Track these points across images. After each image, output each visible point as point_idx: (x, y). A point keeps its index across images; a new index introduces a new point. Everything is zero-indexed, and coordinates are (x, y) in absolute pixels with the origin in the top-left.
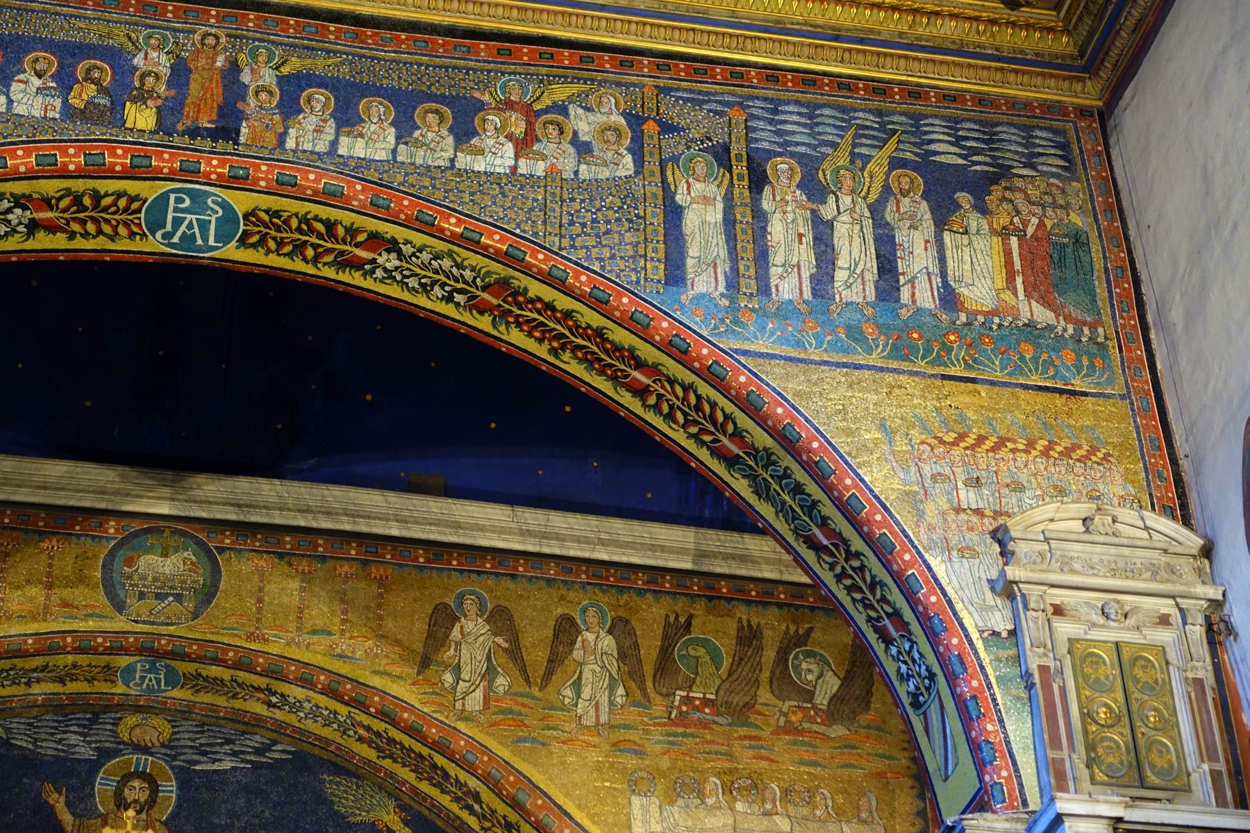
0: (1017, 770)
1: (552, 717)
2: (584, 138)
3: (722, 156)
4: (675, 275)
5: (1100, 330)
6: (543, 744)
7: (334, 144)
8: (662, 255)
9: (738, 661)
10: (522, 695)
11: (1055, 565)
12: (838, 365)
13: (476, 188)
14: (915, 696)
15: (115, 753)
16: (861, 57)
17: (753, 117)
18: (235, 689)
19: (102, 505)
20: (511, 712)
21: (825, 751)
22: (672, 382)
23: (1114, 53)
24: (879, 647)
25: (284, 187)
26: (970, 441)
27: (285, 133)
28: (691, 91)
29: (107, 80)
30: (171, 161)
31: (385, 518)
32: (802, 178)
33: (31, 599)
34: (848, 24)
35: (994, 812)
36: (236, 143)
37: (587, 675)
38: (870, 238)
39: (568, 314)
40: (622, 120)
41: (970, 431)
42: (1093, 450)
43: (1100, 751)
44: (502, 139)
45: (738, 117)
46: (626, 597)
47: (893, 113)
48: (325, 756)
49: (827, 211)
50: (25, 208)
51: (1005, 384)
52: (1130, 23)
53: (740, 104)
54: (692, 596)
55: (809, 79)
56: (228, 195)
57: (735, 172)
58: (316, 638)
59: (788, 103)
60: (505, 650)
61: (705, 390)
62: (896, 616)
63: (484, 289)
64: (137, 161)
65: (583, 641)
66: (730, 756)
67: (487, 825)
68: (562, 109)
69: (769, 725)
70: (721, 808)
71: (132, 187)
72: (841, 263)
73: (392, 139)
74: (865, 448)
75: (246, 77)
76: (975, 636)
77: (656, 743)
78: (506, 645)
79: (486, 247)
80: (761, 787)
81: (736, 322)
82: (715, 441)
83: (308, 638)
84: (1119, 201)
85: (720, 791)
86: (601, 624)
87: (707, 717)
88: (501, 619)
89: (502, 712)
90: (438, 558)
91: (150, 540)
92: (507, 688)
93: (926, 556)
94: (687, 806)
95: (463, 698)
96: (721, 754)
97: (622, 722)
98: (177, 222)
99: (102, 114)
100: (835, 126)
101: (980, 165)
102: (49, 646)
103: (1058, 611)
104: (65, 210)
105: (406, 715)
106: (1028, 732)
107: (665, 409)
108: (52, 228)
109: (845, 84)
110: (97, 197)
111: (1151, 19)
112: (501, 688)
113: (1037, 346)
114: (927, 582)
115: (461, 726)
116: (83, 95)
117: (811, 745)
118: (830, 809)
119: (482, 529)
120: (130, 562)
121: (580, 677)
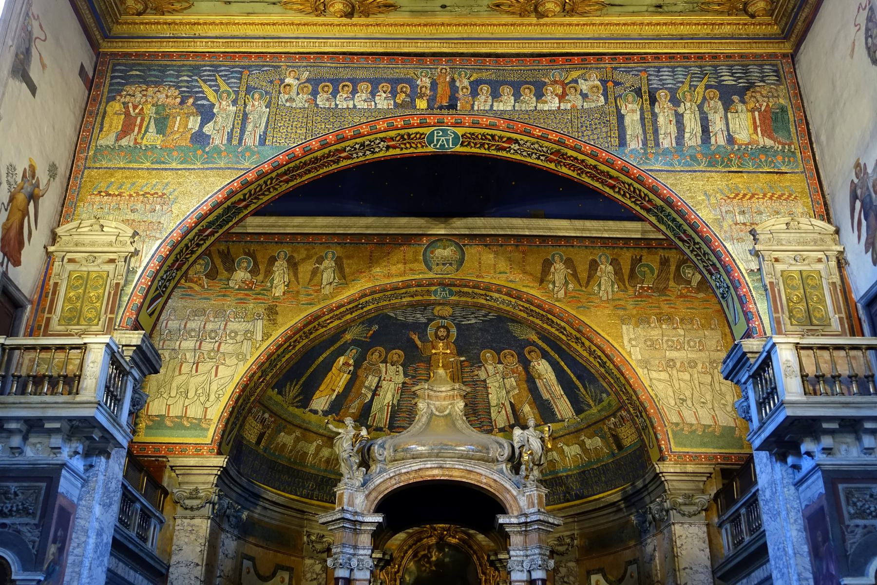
0: (762, 322)
2: (586, 92)
3: (638, 92)
4: (623, 143)
5: (793, 146)
7: (492, 106)
8: (617, 135)
9: (661, 271)
10: (579, 291)
11: (775, 243)
12: (687, 171)
13: (545, 117)
14: (723, 294)
15: (433, 320)
16: (692, 45)
17: (650, 75)
18: (473, 295)
19: (421, 232)
20: (575, 297)
21: (696, 303)
22: (624, 183)
23: (796, 31)
24: (708, 276)
25: (475, 125)
26: (740, 196)
27: (473, 104)
28: (625, 67)
29: (408, 92)
30: (434, 119)
31: (523, 228)
32: (671, 97)
33: (399, 269)
34: (686, 33)
35: (753, 338)
36: (456, 110)
37: (603, 281)
38: (698, 119)
39: (583, 161)
40: (599, 83)
41: (740, 192)
42: (790, 195)
43: (794, 312)
44: (554, 96)
45: (644, 76)
46: (616, 250)
47: (706, 66)
48: (508, 316)
49: (681, 110)
50: (384, 142)
51: (754, 172)
52: (802, 19)
53: (645, 70)
54: (641, 248)
55: (671, 56)
56: (456, 130)
57: (644, 98)
58: (501, 275)
59: (663, 67)
60: (571, 274)
61: (636, 185)
62: (714, 265)
63: (551, 154)
64: (422, 121)
66: (659, 308)
68: (576, 81)
69: (674, 295)
71: (421, 130)
72: (687, 130)
73: (513, 101)
74: (699, 203)
75: (458, 84)
76: (744, 272)
79: (551, 139)
81: (647, 159)
82: (642, 203)
83: (498, 275)
84: (800, 91)
86: (607, 262)
88: (569, 263)
89: (572, 297)
90: (544, 241)
91: (439, 244)
93: (724, 243)
98: (438, 141)
99: (408, 104)
100: (683, 75)
101: (742, 83)
102: (407, 285)
103: (777, 260)
104: (399, 141)
106: (766, 307)
107: (622, 192)
108: (394, 147)
109: (686, 57)
110: (409, 135)
111: (810, 17)
113: (767, 155)
114: (725, 253)
115: (557, 303)
119: (559, 229)
120: (432, 252)
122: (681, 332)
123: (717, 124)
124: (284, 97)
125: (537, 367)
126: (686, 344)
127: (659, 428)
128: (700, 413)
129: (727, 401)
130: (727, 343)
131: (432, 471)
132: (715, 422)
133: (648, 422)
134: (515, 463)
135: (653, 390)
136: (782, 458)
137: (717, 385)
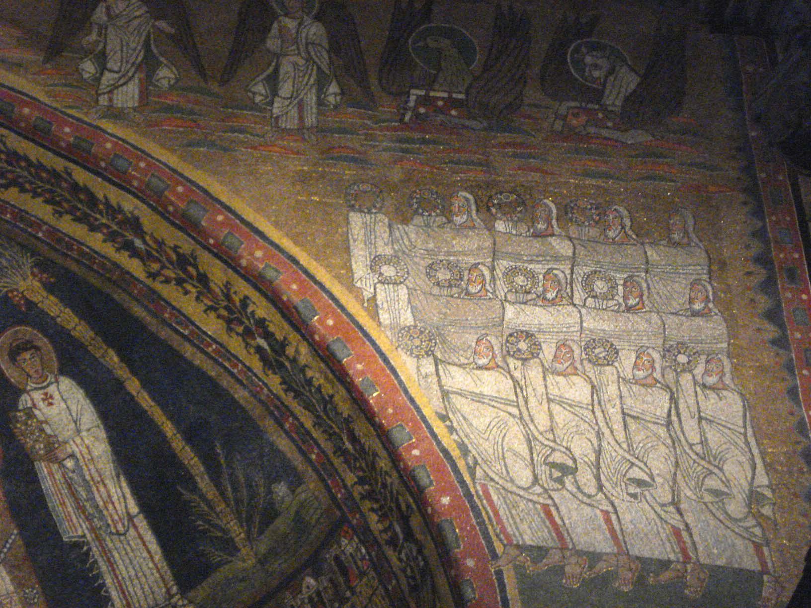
1: (236, 116)
6: (225, 150)
37: (286, 68)
60: (171, 37)
65: (280, 30)
66: (486, 165)
67: (155, 267)
70: (474, 227)
77: (384, 150)
78: (173, 31)
80: (529, 203)
85: (474, 207)
87: (457, 120)
89: (168, 109)
92: (172, 82)
94: (427, 225)
95: (111, 92)
96: (473, 163)
97: (336, 125)
105: (26, 111)
112: (165, 83)
115: (108, 126)
117: (600, 154)
118: (627, 228)
121: (276, 70)
122: (564, 248)
125: (43, 411)
126: (578, 287)
127: (470, 563)
128: (626, 517)
129: (727, 483)
130: (728, 289)
132: (684, 551)
133: (430, 548)
135: (451, 429)
137: (690, 427)
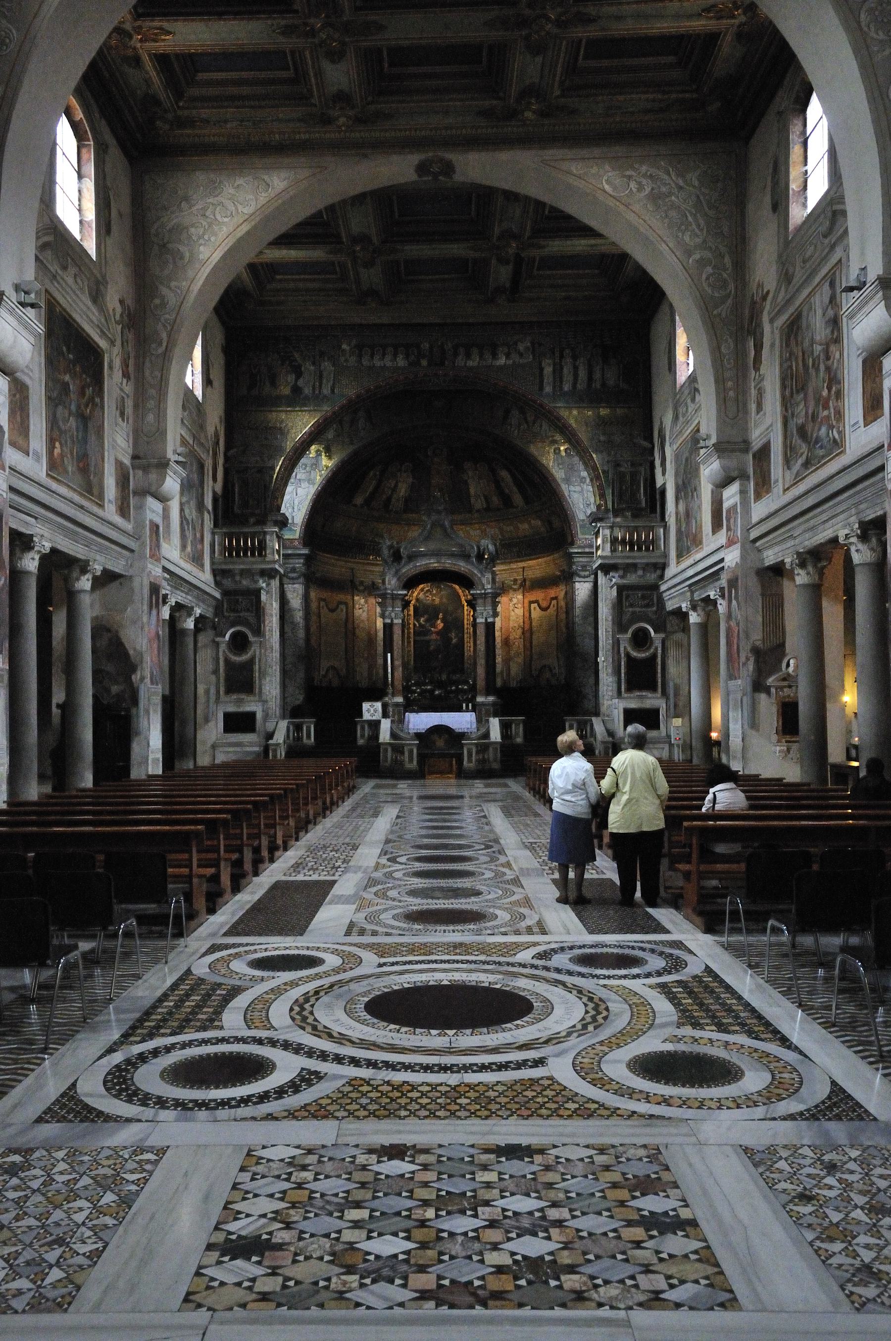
4: (541, 388)
68: (516, 343)
116: (412, 358)
123: (597, 375)
124: (342, 359)
131: (433, 564)
134: (480, 557)
136: (606, 574)
